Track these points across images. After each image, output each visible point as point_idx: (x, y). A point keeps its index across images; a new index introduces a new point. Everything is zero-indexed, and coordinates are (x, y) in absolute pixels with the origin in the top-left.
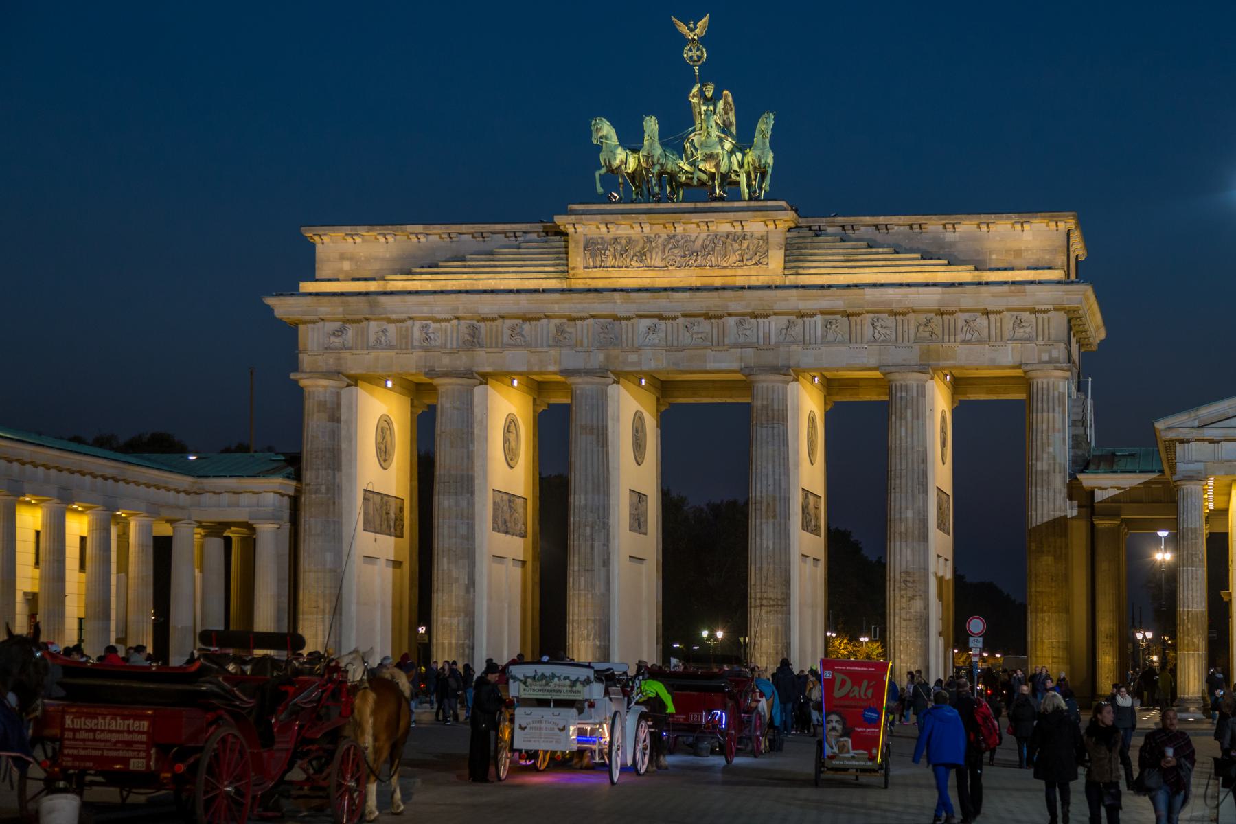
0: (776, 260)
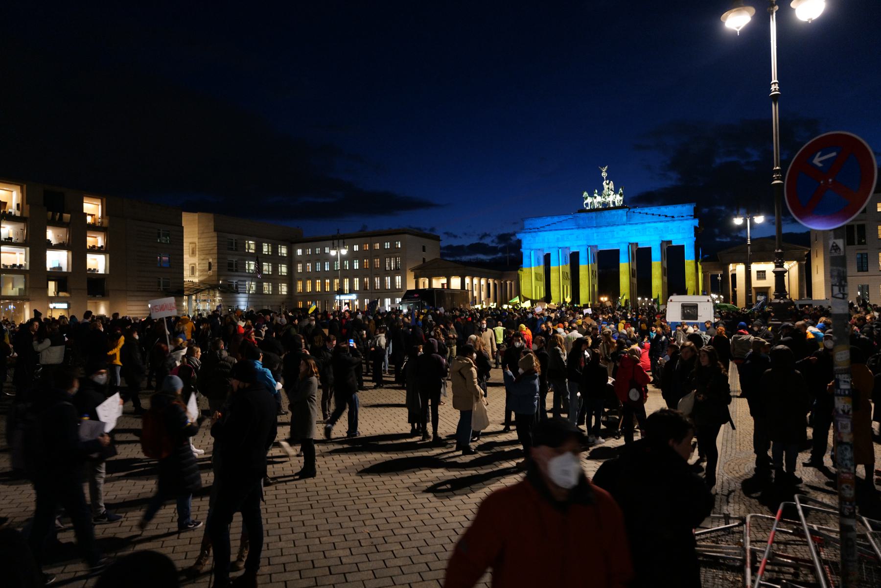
0: (625, 218)
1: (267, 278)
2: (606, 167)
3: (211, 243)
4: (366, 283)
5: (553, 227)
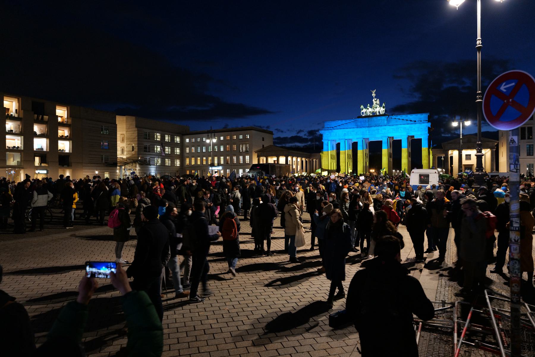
0: (386, 122)
1: (168, 156)
2: (375, 90)
3: (133, 135)
4: (227, 159)
5: (342, 127)
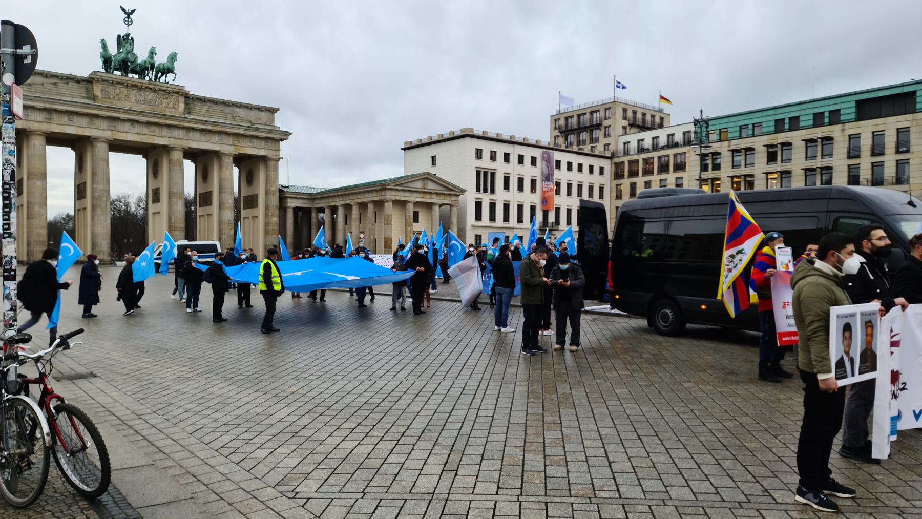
0: (182, 106)
